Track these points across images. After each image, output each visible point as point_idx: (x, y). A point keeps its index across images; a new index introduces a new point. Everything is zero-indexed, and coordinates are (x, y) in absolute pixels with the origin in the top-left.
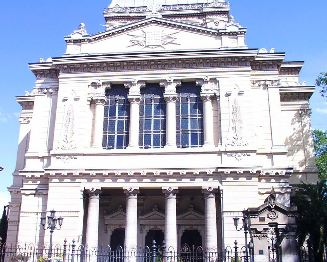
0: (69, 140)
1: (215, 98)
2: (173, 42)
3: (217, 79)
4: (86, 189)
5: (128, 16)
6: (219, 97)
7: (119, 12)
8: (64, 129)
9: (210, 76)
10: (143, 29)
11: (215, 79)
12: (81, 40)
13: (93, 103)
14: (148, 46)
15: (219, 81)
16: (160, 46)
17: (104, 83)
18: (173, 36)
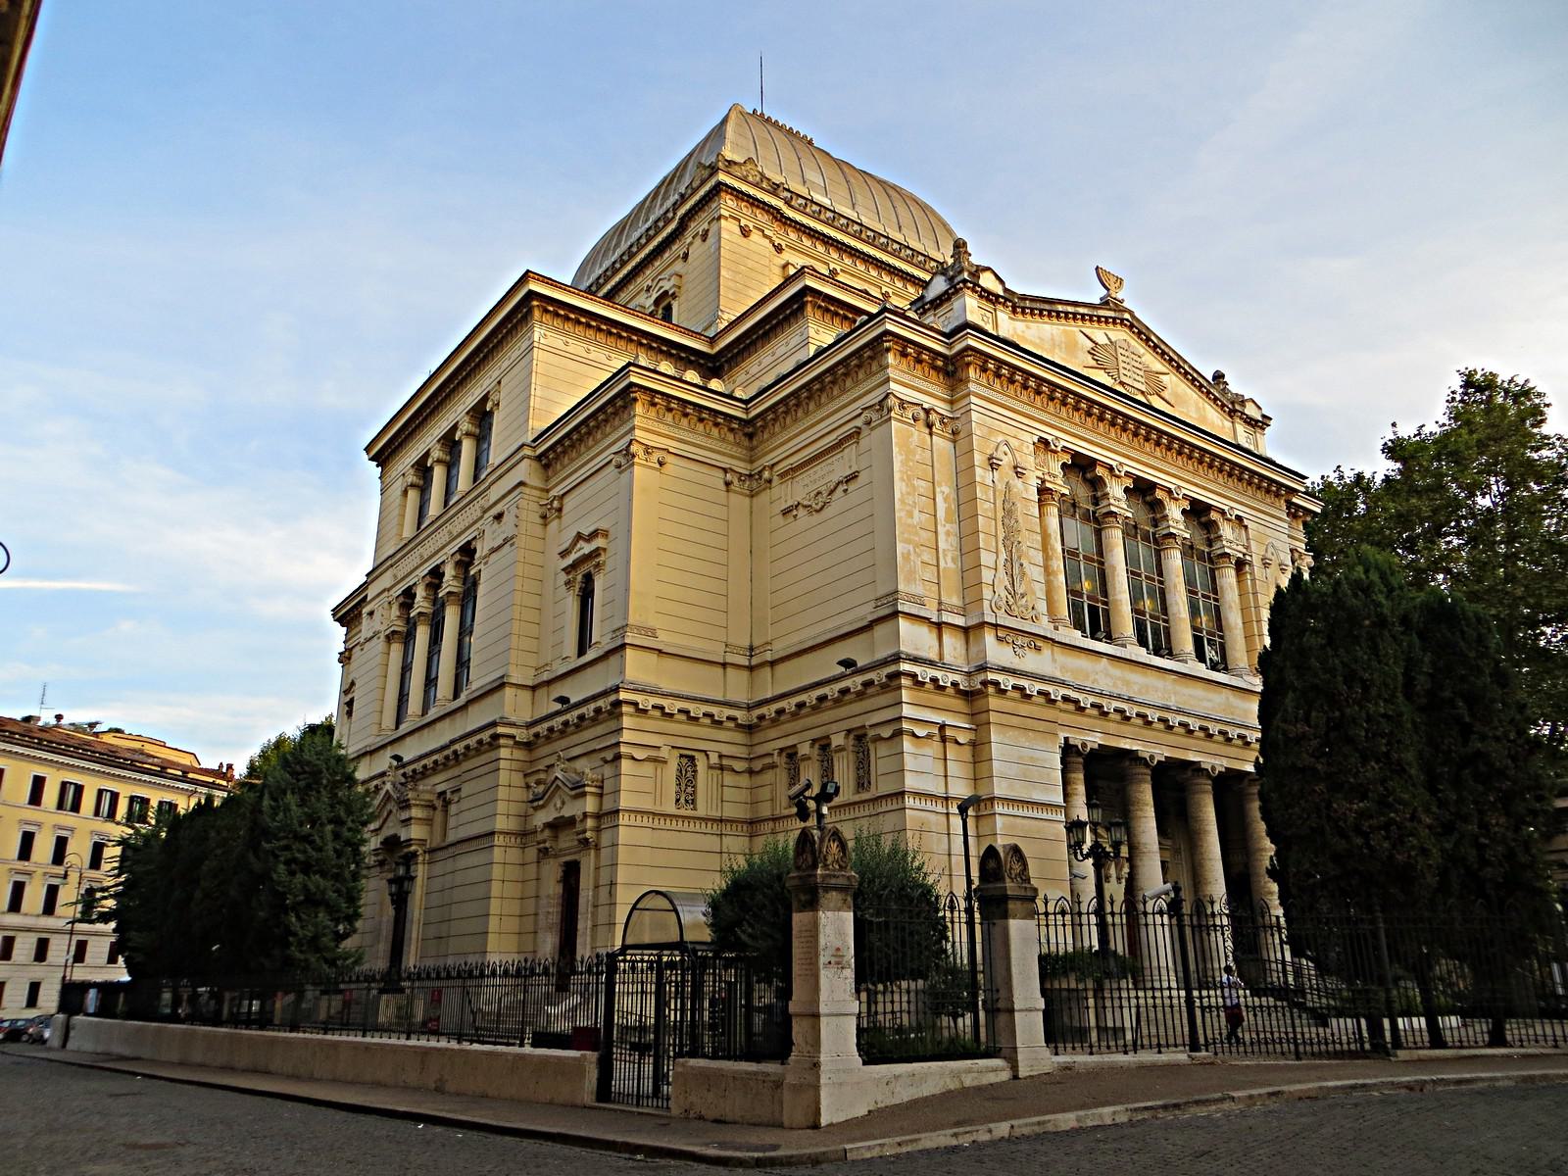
0: (1020, 590)
1: (1240, 565)
2: (1162, 394)
3: (1246, 522)
4: (1071, 742)
5: (778, 211)
6: (1250, 564)
7: (756, 185)
8: (1003, 556)
9: (1240, 510)
10: (1110, 334)
11: (1239, 518)
12: (997, 296)
13: (1043, 491)
14: (1122, 383)
15: (1246, 527)
16: (1143, 393)
17: (1065, 450)
18: (1161, 376)
